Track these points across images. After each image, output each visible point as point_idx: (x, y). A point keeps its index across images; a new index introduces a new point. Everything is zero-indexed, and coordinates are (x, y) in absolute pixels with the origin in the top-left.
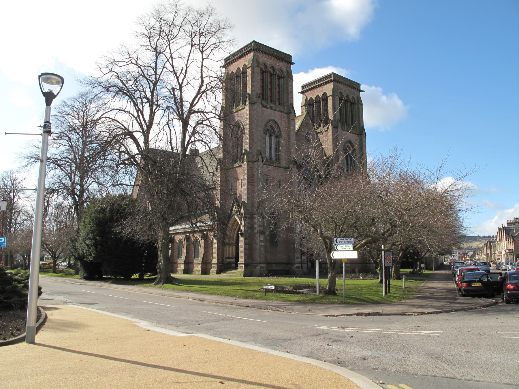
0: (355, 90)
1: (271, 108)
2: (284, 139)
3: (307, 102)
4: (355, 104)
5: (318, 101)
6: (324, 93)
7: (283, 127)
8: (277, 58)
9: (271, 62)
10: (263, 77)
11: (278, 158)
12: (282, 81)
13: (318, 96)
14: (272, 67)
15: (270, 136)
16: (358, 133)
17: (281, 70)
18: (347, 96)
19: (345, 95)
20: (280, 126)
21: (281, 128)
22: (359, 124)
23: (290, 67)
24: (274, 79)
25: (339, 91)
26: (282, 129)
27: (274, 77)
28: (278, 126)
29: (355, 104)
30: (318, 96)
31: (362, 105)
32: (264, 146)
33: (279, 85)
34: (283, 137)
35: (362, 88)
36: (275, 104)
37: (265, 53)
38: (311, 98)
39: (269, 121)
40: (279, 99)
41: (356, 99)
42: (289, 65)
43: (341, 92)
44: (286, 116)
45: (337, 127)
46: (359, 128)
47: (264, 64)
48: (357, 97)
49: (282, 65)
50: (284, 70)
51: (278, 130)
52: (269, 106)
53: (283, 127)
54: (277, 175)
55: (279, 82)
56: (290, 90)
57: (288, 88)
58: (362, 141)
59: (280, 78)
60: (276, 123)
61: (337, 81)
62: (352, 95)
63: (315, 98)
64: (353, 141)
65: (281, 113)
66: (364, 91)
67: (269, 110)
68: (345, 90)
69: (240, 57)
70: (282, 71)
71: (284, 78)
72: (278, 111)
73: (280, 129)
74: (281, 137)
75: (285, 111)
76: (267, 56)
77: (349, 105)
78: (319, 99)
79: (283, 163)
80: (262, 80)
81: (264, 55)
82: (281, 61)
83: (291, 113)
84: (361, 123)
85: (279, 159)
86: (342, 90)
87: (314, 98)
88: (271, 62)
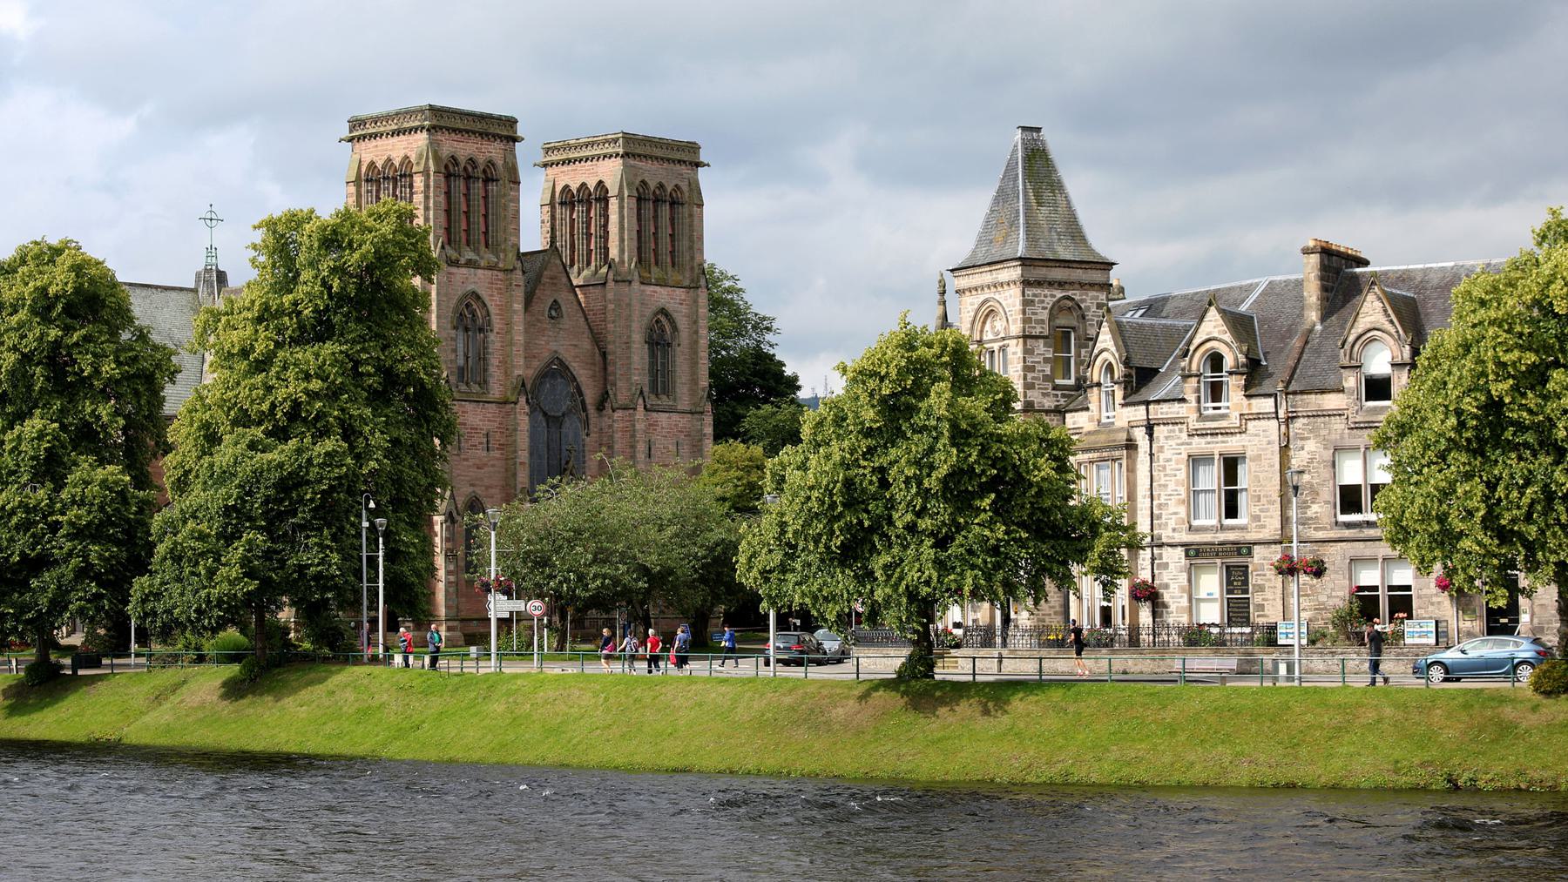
0: (683, 167)
1: (470, 264)
2: (498, 333)
3: (557, 195)
4: (682, 204)
5: (585, 197)
6: (600, 182)
7: (496, 305)
8: (481, 134)
9: (465, 148)
10: (449, 187)
11: (484, 383)
12: (492, 187)
13: (583, 185)
14: (471, 159)
15: (466, 330)
16: (687, 283)
17: (491, 163)
18: (661, 186)
19: (652, 185)
20: (488, 303)
21: (490, 308)
22: (692, 258)
23: (513, 151)
24: (474, 189)
25: (640, 179)
26: (493, 310)
27: (474, 183)
28: (485, 305)
29: (682, 204)
30: (583, 185)
31: (701, 205)
32: (453, 357)
33: (486, 198)
34: (496, 330)
35: (703, 158)
36: (476, 251)
37: (454, 130)
38: (566, 188)
39: (465, 296)
40: (486, 233)
41: (685, 188)
42: (511, 143)
43: (644, 182)
44: (501, 275)
45: (630, 282)
46: (692, 268)
47: (452, 157)
48: (690, 184)
49: (494, 150)
50: (500, 163)
51: (484, 313)
52: (463, 261)
53: (496, 305)
54: (480, 420)
55: (486, 191)
56: (510, 213)
57: (505, 208)
58: (697, 306)
59: (487, 181)
60: (478, 297)
61: (633, 155)
62: (675, 182)
63: (579, 191)
64: (671, 306)
65: (490, 272)
66: (708, 165)
67: (464, 270)
68: (654, 173)
69: (393, 133)
70: (493, 165)
71: (497, 180)
72: (484, 268)
73: (488, 311)
74: (491, 331)
75: (501, 265)
76: (459, 136)
77: (665, 210)
78: (587, 192)
79: (496, 391)
80: (448, 194)
81: (453, 135)
82: (492, 139)
83: (515, 269)
84: (697, 256)
85: (485, 382)
86: (646, 174)
87: (574, 187)
88: (465, 148)
